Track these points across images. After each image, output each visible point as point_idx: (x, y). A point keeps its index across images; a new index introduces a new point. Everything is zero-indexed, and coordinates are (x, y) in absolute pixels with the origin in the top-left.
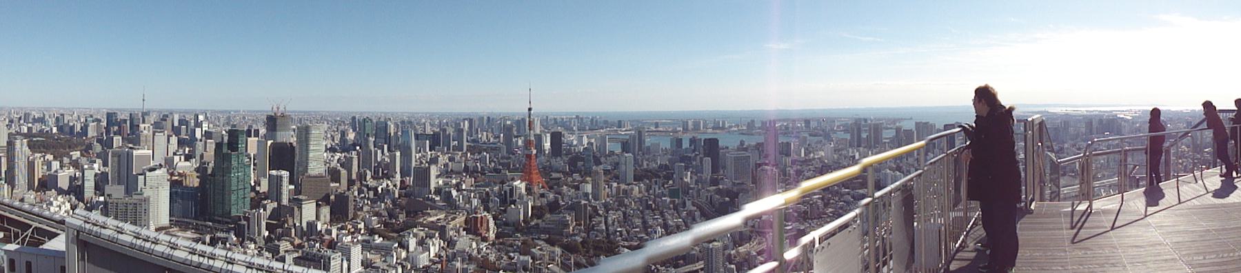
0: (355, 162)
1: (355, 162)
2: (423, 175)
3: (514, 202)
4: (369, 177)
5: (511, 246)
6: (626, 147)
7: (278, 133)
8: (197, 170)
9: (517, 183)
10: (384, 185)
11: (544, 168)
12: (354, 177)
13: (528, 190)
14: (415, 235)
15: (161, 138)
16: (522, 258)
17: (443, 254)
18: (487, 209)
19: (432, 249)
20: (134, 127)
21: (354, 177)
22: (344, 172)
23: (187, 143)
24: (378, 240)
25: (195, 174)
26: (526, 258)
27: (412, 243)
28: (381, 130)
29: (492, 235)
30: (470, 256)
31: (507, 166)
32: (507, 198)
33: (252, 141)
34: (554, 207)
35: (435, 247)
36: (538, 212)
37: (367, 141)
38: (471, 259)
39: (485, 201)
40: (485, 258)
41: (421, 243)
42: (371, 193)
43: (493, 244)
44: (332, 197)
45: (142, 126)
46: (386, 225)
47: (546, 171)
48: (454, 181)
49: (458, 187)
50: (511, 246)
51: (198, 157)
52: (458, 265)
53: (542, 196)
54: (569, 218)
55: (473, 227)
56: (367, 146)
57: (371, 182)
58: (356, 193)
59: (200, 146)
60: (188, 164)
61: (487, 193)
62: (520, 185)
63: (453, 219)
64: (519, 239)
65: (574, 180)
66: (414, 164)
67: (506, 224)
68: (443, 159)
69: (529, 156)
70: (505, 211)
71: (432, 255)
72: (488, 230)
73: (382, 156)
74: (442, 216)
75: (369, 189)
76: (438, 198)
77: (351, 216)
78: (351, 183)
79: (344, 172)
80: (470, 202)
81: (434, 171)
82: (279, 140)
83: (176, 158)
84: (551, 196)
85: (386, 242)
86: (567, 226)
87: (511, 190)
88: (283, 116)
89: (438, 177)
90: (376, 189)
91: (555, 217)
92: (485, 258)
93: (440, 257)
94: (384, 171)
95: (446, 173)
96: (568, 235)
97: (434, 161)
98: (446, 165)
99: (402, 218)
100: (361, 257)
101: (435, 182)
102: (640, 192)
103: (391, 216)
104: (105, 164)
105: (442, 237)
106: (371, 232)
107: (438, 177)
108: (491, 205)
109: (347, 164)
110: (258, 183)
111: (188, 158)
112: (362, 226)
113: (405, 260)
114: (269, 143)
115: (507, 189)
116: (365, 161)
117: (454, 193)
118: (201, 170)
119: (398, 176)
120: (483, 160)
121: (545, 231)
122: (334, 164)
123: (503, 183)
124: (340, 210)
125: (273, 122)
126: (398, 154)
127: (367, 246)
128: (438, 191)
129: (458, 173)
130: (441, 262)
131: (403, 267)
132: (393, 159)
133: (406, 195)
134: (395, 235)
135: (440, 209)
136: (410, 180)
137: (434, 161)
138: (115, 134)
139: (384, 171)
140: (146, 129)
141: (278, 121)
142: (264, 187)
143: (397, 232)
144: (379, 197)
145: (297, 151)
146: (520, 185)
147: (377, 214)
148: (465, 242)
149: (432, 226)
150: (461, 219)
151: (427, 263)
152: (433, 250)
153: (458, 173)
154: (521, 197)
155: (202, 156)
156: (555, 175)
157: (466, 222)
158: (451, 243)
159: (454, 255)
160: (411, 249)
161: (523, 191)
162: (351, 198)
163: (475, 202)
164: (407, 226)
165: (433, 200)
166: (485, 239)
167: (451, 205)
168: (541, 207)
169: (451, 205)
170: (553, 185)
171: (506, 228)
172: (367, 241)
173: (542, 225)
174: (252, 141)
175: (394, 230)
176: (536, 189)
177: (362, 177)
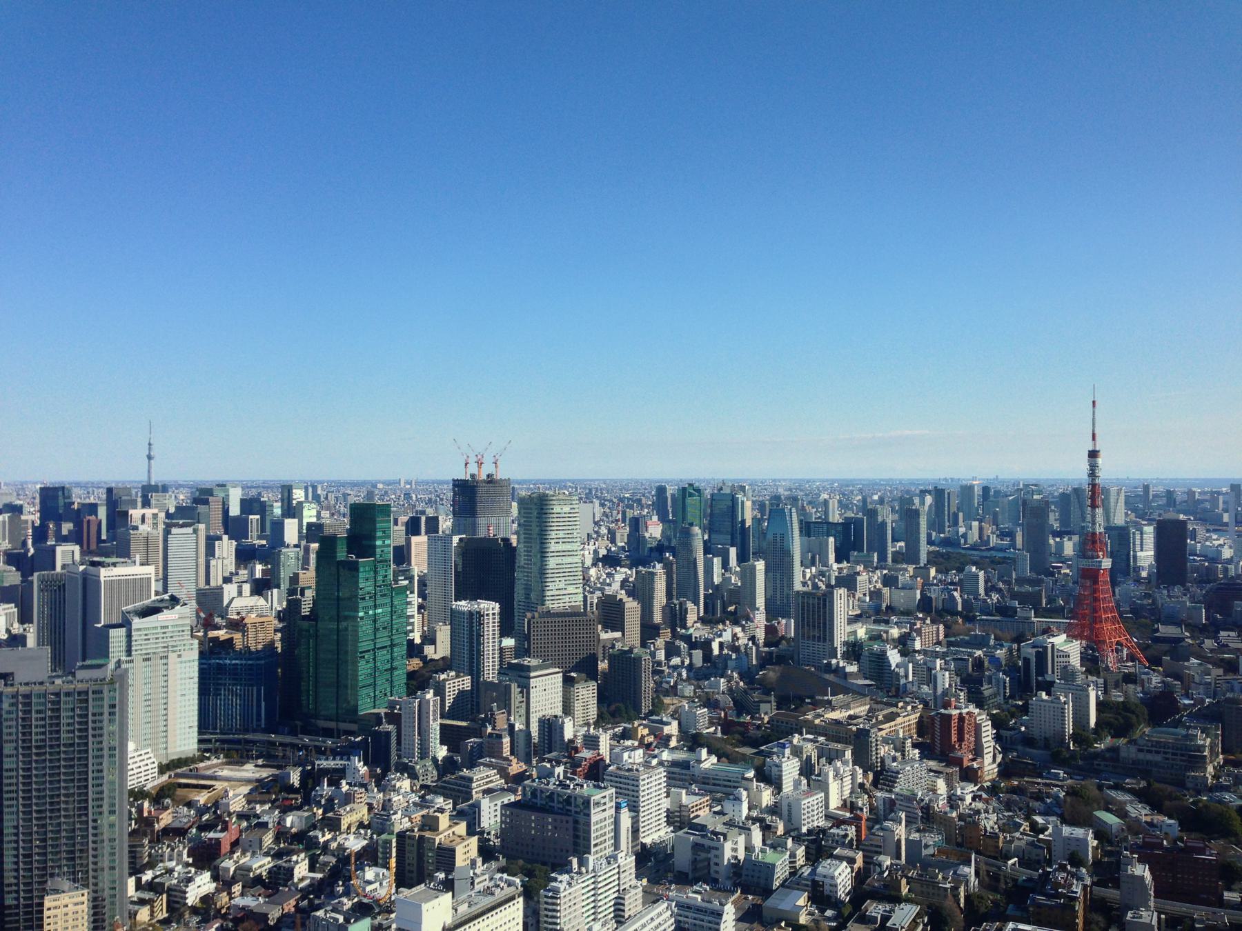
0: (660, 586)
1: (660, 586)
2: (816, 611)
3: (1048, 687)
4: (691, 618)
5: (1038, 797)
7: (481, 521)
8: (281, 616)
9: (1059, 640)
10: (727, 636)
11: (1136, 611)
12: (658, 618)
13: (1092, 662)
14: (797, 752)
15: (185, 541)
16: (1066, 830)
17: (862, 801)
18: (980, 705)
19: (834, 787)
20: (118, 517)
21: (658, 618)
22: (631, 605)
23: (259, 556)
24: (708, 761)
25: (276, 624)
26: (1079, 832)
27: (790, 769)
28: (721, 512)
29: (989, 766)
30: (927, 809)
31: (1031, 601)
32: (1030, 676)
33: (419, 542)
34: (1161, 708)
35: (841, 783)
36: (1116, 718)
37: (687, 534)
38: (927, 817)
39: (972, 683)
40: (970, 821)
41: (807, 770)
42: (698, 654)
43: (993, 790)
44: (603, 665)
45: (135, 513)
46: (727, 727)
47: (1141, 617)
48: (895, 632)
49: (903, 644)
50: (1038, 797)
51: (285, 585)
52: (901, 831)
53: (1130, 679)
54: (1203, 740)
55: (937, 741)
56: (688, 547)
57: (697, 631)
58: (661, 655)
59: (289, 559)
60: (261, 601)
61: (979, 663)
62: (1067, 647)
63: (891, 718)
64: (1060, 783)
65: (1223, 647)
66: (798, 587)
67: (1028, 741)
68: (867, 580)
69: (1091, 575)
70: (1025, 709)
71: (834, 803)
72: (978, 752)
73: (720, 572)
74: (861, 709)
75: (693, 644)
76: (852, 668)
77: (646, 706)
78: (649, 631)
79: (632, 606)
80: (931, 680)
81: (843, 606)
82: (481, 534)
83: (230, 591)
84: (1155, 680)
85: (726, 767)
86: (1197, 761)
87: (1041, 656)
88: (490, 480)
89: (853, 620)
90: (706, 645)
91: (1166, 735)
92: (970, 821)
93: (853, 807)
94: (726, 606)
95: (876, 612)
96: (1202, 787)
97: (848, 582)
98: (875, 594)
99: (767, 713)
100: (666, 804)
101: (842, 632)
103: (741, 706)
104: (25, 618)
105: (861, 758)
106: (693, 741)
107: (853, 620)
108: (987, 690)
109: (641, 591)
110: (429, 639)
111: (260, 587)
112: (672, 729)
113: (774, 810)
114: (456, 539)
115: (1029, 651)
116: (682, 585)
117: (894, 657)
118: (289, 615)
119: (760, 618)
120: (968, 585)
121: (1137, 769)
122: (615, 588)
123: (1019, 639)
124: (620, 696)
125: (468, 496)
126: (760, 565)
127: (680, 775)
128: (854, 650)
129: (907, 613)
130: (856, 821)
131: (766, 829)
132: (748, 576)
133: (780, 660)
134: (748, 751)
135: (859, 693)
136: (788, 626)
137: (848, 582)
138: (63, 539)
139: (726, 606)
140: (145, 521)
141: (481, 492)
142: (441, 649)
143: (754, 743)
144: (714, 666)
145: (521, 560)
146: (1067, 647)
147: (710, 703)
148: (918, 777)
149: (836, 732)
150: (907, 720)
151: (822, 823)
152: (837, 793)
153: (907, 613)
154: (1068, 674)
155: (294, 579)
156: (1165, 630)
157: (921, 727)
158: (883, 777)
159: (891, 806)
160: (788, 786)
161: (1075, 661)
162: (647, 665)
163: (945, 680)
164: (779, 732)
165: (838, 671)
166: (970, 775)
167: (886, 688)
168: (1125, 707)
169: (886, 688)
170: (1160, 652)
171: (1028, 753)
172: (685, 765)
173: (1129, 752)
174: (419, 542)
175: (748, 740)
176: (1111, 660)
177: (676, 618)
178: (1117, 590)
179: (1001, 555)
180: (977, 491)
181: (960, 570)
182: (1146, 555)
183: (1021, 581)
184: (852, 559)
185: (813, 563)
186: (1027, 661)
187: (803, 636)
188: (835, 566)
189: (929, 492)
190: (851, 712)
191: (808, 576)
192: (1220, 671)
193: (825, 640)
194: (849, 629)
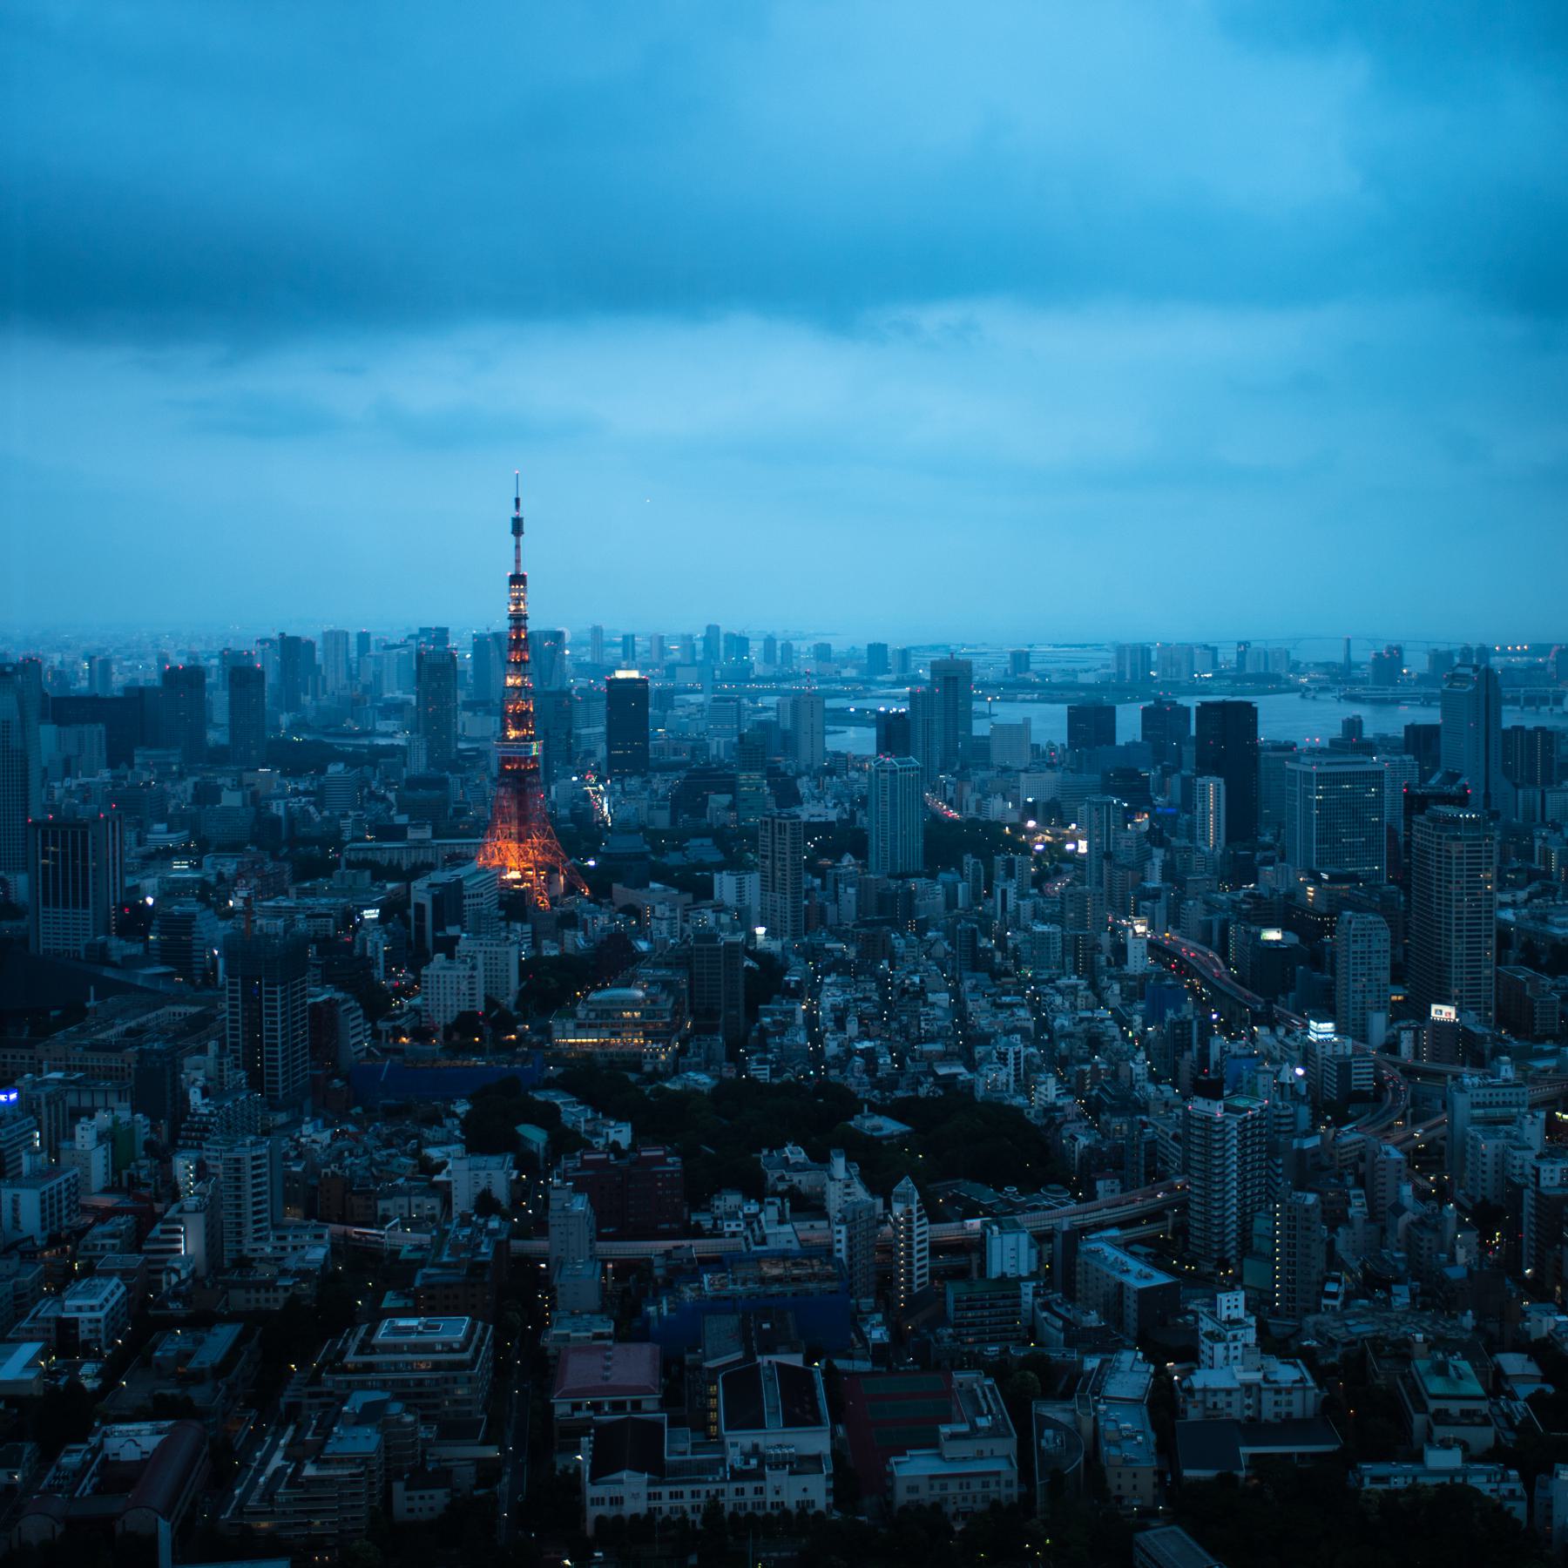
6: (893, 733)
102: (951, 902)
115: (420, 891)
168: (564, 963)
178: (553, 789)
179: (382, 742)
180: (353, 640)
181: (323, 771)
182: (593, 731)
183: (414, 783)
184: (137, 760)
185: (67, 772)
186: (420, 908)
187: (46, 903)
188: (105, 774)
189: (271, 641)
190: (132, 1024)
191: (57, 793)
192: (688, 897)
193: (85, 905)
194: (129, 882)
